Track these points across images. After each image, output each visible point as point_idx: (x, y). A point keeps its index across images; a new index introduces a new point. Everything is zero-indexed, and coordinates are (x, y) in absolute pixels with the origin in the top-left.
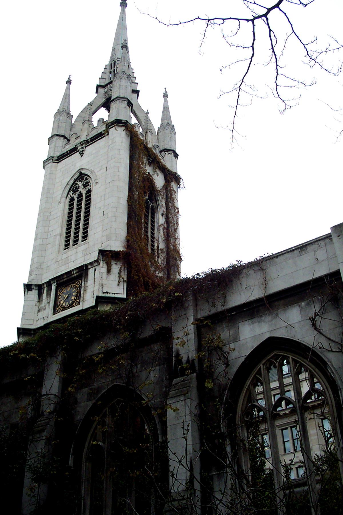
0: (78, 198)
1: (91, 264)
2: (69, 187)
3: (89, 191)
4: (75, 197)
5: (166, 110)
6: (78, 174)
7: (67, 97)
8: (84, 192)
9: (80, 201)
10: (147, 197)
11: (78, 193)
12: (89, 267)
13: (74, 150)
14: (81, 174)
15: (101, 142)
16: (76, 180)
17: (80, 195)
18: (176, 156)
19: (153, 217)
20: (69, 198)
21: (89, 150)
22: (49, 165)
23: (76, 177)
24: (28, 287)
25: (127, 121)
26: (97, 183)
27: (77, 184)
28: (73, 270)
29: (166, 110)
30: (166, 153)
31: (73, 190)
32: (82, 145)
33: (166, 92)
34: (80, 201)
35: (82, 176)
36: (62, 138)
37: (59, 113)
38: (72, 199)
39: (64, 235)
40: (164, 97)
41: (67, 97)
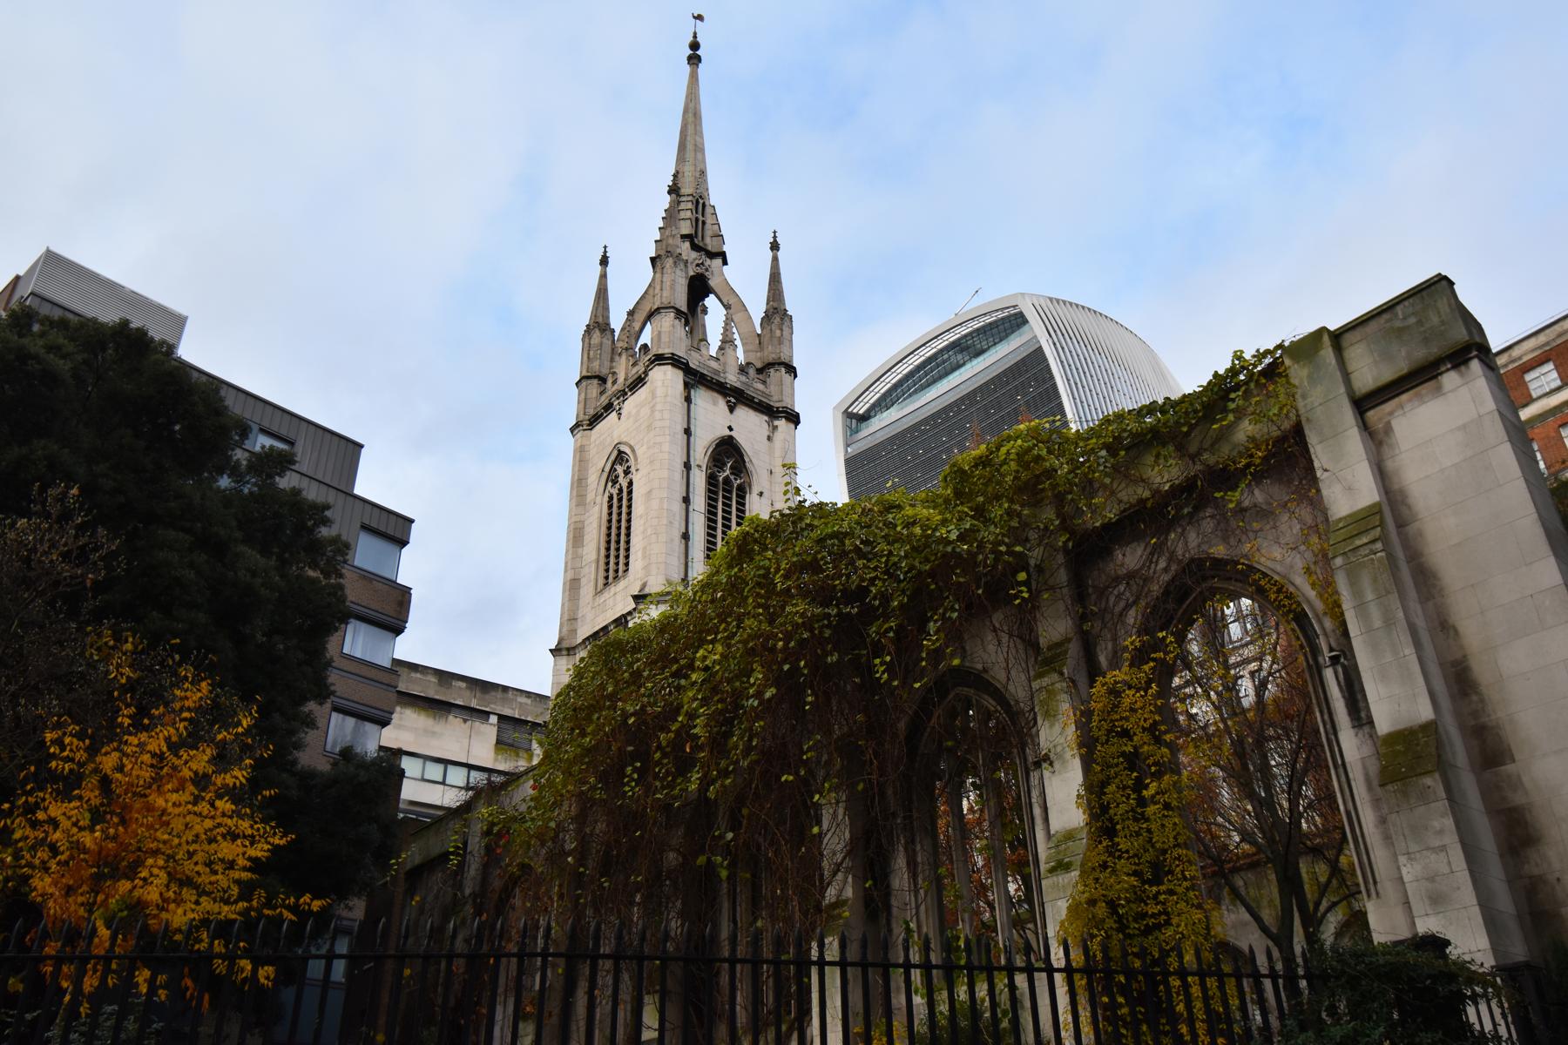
0: (618, 495)
1: (630, 613)
2: (605, 475)
3: (631, 484)
4: (615, 492)
5: (775, 278)
6: (615, 453)
7: (602, 294)
8: (625, 485)
9: (620, 500)
10: (728, 472)
11: (617, 486)
12: (629, 618)
13: (609, 408)
14: (620, 452)
15: (642, 393)
16: (614, 464)
17: (621, 490)
18: (792, 370)
19: (741, 504)
20: (607, 494)
21: (632, 403)
22: (579, 435)
23: (613, 457)
24: (556, 652)
25: (672, 354)
26: (637, 470)
27: (615, 470)
28: (609, 624)
29: (775, 278)
30: (772, 370)
31: (612, 481)
32: (618, 398)
33: (775, 241)
34: (620, 500)
35: (620, 457)
36: (595, 381)
37: (589, 330)
38: (611, 497)
39: (602, 560)
40: (772, 249)
41: (602, 294)
